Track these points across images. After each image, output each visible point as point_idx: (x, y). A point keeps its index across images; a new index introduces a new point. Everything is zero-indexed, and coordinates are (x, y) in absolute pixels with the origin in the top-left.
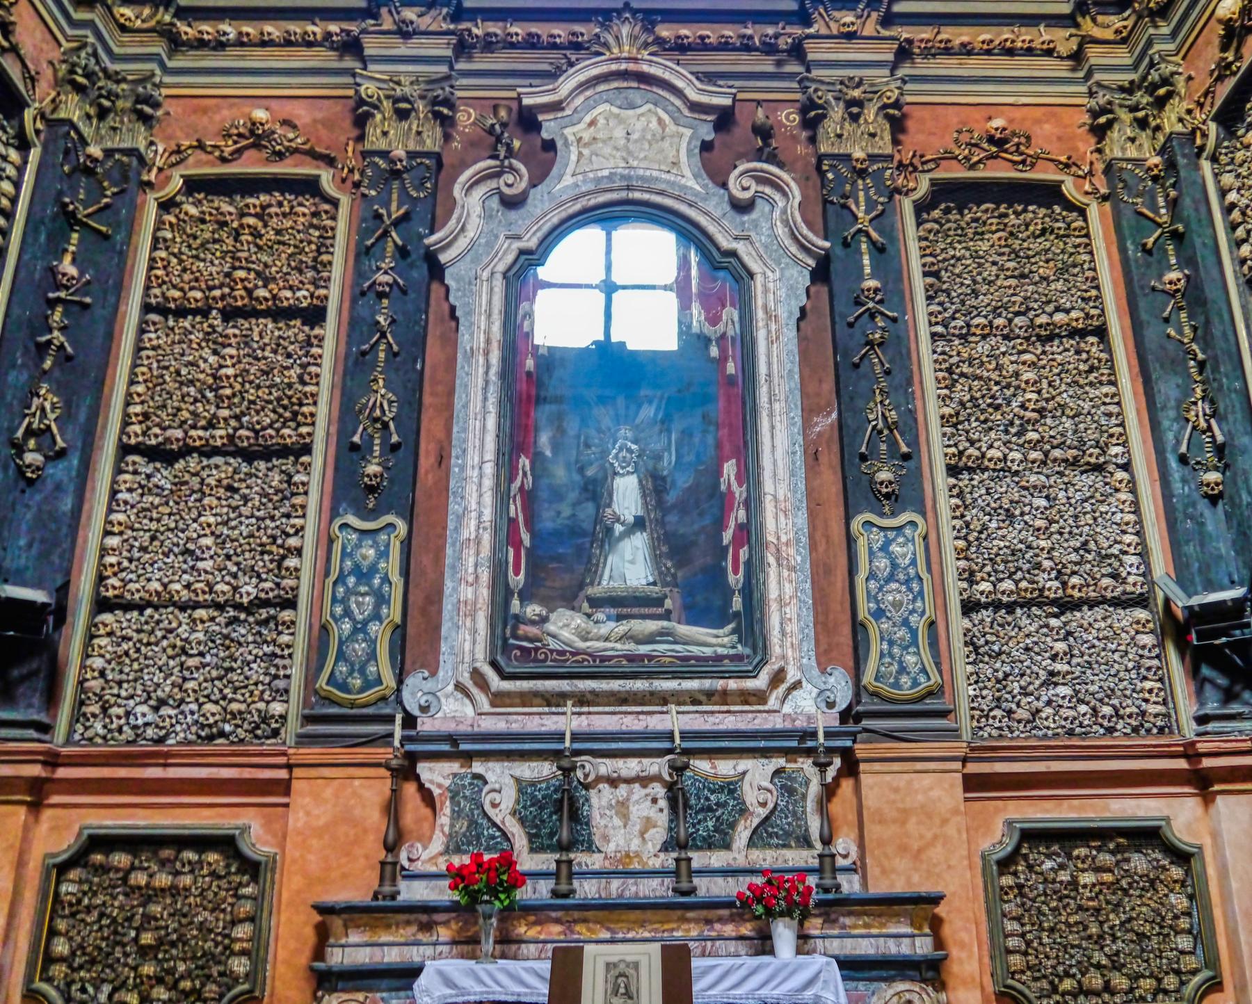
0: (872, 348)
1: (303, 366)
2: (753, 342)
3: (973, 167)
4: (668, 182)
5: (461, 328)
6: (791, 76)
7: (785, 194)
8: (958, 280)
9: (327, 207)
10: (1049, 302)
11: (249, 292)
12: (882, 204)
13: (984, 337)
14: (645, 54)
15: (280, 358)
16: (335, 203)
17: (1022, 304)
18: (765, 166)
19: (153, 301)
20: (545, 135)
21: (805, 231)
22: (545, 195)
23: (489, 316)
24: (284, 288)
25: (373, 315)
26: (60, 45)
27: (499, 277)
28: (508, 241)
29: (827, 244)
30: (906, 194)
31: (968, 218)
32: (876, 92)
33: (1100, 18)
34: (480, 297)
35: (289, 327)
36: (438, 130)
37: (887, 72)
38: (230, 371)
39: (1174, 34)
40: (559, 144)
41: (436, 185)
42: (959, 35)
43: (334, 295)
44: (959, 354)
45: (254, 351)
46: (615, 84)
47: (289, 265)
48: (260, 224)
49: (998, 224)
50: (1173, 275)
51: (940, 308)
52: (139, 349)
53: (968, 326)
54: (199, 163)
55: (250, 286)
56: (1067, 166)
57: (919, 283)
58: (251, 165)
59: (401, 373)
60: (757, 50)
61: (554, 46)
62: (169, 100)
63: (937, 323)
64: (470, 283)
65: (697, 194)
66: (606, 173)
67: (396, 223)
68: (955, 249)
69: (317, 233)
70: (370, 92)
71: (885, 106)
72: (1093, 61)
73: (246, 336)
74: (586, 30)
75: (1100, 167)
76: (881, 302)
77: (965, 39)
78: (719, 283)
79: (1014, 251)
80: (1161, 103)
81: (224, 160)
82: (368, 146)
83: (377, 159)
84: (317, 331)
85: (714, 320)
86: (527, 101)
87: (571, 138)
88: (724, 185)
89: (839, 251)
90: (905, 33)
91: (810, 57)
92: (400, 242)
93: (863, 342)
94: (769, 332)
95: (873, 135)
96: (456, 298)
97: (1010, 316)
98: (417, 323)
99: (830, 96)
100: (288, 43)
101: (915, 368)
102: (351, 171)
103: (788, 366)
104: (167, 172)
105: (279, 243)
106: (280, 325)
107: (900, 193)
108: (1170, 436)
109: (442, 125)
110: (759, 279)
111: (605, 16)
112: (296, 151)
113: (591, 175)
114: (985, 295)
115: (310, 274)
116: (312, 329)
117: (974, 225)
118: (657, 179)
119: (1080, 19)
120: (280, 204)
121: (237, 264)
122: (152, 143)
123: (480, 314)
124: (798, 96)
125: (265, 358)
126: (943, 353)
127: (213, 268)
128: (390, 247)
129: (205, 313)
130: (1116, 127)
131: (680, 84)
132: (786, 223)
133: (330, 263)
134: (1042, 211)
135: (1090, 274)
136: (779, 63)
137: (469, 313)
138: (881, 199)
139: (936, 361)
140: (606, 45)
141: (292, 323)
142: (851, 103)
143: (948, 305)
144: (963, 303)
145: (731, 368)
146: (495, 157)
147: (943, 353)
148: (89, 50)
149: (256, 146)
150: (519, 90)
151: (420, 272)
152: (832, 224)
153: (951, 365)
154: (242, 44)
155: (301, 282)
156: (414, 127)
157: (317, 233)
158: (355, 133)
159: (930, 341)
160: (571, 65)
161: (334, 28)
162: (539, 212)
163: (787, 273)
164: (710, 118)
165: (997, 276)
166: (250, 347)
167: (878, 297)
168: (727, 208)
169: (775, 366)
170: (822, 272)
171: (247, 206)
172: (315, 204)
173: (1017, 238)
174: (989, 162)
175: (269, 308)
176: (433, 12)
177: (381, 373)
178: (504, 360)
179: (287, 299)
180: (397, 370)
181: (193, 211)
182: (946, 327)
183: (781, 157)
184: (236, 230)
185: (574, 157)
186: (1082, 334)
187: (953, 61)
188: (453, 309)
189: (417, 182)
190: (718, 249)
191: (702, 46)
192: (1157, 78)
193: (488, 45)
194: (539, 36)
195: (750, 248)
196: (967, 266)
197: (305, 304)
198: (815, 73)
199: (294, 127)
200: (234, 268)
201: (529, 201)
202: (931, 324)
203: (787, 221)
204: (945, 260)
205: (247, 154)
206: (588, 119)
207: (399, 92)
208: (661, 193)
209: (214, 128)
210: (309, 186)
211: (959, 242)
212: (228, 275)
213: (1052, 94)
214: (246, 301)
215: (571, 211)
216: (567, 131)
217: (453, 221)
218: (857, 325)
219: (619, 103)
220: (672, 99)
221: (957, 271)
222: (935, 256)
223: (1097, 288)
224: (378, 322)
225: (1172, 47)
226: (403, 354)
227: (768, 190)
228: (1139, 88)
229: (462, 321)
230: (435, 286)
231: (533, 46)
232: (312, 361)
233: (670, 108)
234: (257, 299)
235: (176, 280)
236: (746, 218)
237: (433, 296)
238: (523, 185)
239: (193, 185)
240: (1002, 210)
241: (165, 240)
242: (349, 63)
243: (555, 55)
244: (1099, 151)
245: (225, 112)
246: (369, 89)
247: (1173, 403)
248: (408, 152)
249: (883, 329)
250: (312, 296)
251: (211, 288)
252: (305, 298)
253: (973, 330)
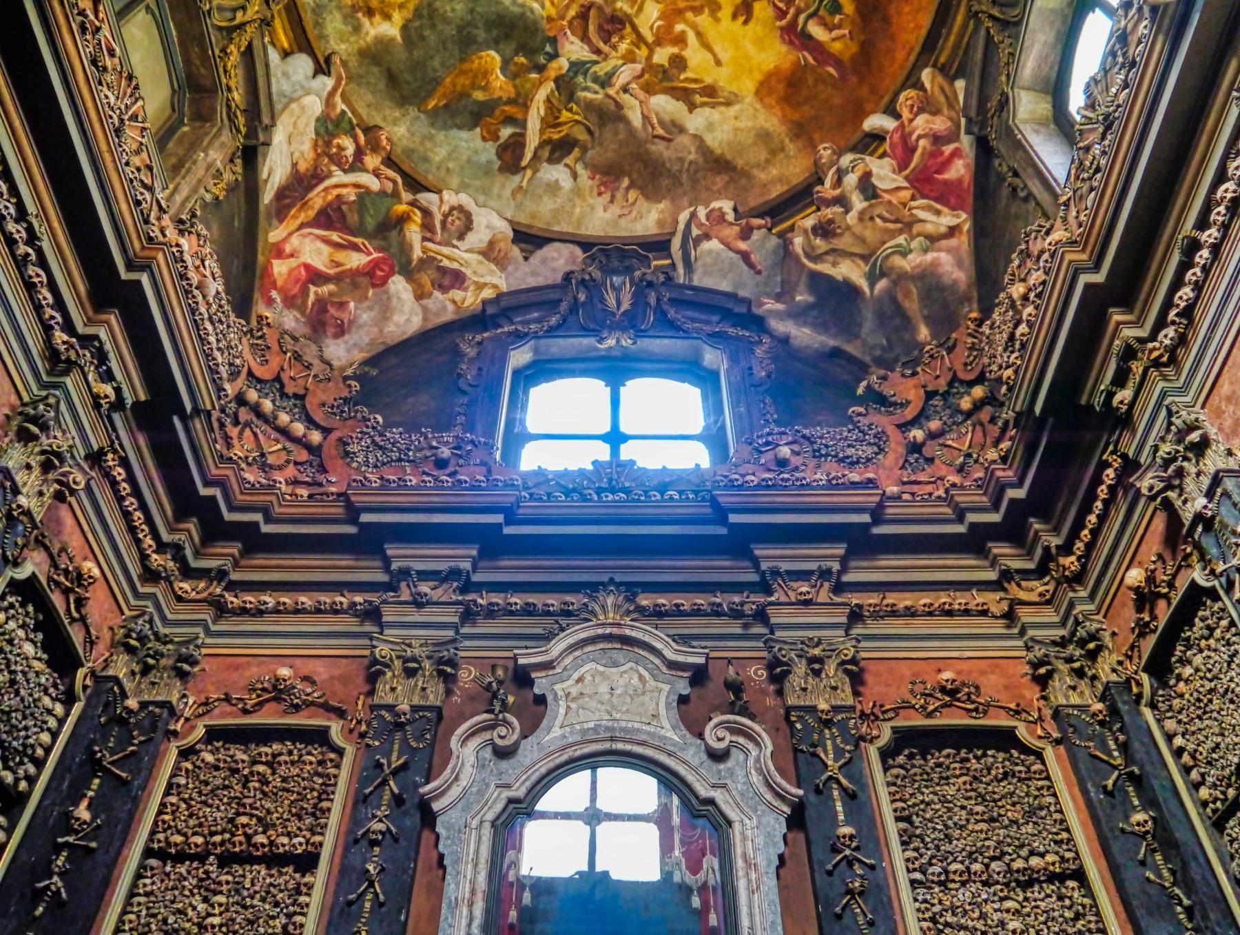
0: (853, 898)
1: (289, 916)
2: (734, 891)
3: (930, 715)
4: (649, 733)
5: (448, 877)
6: (757, 637)
7: (757, 744)
8: (930, 825)
9: (332, 756)
10: (1022, 846)
11: (248, 837)
12: (849, 752)
13: (963, 884)
14: (627, 620)
15: (267, 907)
16: (340, 752)
17: (996, 848)
18: (738, 718)
19: (156, 846)
20: (537, 690)
21: (779, 779)
22: (535, 747)
23: (476, 865)
24: (283, 834)
25: (365, 861)
26: (123, 614)
27: (487, 825)
28: (499, 790)
29: (801, 792)
30: (871, 742)
31: (931, 763)
32: (834, 650)
33: (1023, 583)
34: (468, 845)
35: (281, 874)
36: (441, 687)
37: (842, 633)
38: (216, 920)
39: (1092, 597)
40: (550, 698)
41: (435, 736)
42: (904, 600)
43: (329, 841)
44: (940, 902)
45: (244, 899)
46: (601, 646)
47: (290, 811)
48: (269, 771)
49: (961, 768)
50: (1139, 817)
51: (916, 854)
52: (132, 894)
53: (946, 872)
54: (224, 715)
55: (250, 832)
56: (1017, 712)
57: (892, 829)
58: (268, 717)
59: (385, 924)
60: (725, 615)
61: (548, 614)
62: (207, 658)
63: (915, 870)
64: (460, 831)
65: (675, 744)
66: (591, 725)
67: (395, 773)
68: (923, 794)
69: (320, 781)
70: (383, 653)
71: (843, 663)
72: (1025, 620)
73: (238, 883)
74: (576, 600)
75: (1048, 713)
76: (857, 849)
77: (908, 603)
78: (699, 831)
79: (980, 795)
80: (1093, 656)
81: (245, 712)
82: (377, 701)
83: (383, 713)
84: (308, 879)
85: (695, 868)
86: (521, 661)
87: (560, 693)
88: (700, 736)
89: (812, 798)
90: (855, 599)
91: (773, 620)
92: (396, 791)
93: (843, 890)
94: (749, 881)
95: (835, 688)
96: (445, 846)
97: (986, 861)
98: (405, 872)
99: (793, 654)
100: (318, 611)
101: (898, 918)
102: (359, 722)
103: (771, 917)
104: (192, 723)
105: (284, 790)
106: (273, 872)
107: (865, 741)
109: (445, 682)
110: (737, 827)
111: (592, 588)
112: (312, 704)
113: (578, 727)
114: (958, 840)
115: (309, 821)
116: (303, 876)
117: (938, 770)
118: (638, 730)
119: (1006, 585)
120: (290, 753)
121: (242, 810)
122: (184, 696)
123: (467, 863)
124: (765, 654)
125: (253, 907)
126: (925, 901)
127: (217, 815)
128: (387, 796)
129: (202, 858)
130: (1056, 676)
131: (658, 645)
132: (760, 771)
133: (329, 810)
134: (1001, 756)
135: (1057, 816)
136: (746, 626)
137: (457, 861)
138: (848, 748)
139: (918, 910)
140: (593, 613)
141: (284, 870)
142: (812, 660)
143: (923, 851)
144: (938, 848)
145: (713, 920)
146: (491, 711)
147: (925, 901)
148: (147, 618)
149: (277, 699)
150: (516, 651)
151: (412, 821)
152: (803, 771)
153: (935, 914)
154: (279, 612)
155: (299, 829)
156: (420, 684)
157: (320, 781)
158: (367, 688)
159: (909, 889)
160: (563, 630)
161: (358, 599)
162: (528, 762)
163: (764, 820)
164: (686, 675)
165: (968, 820)
166: (240, 895)
167: (854, 844)
168: (704, 757)
169: (757, 918)
170: (797, 819)
171: (260, 754)
172: (322, 753)
173: (981, 782)
174: (944, 711)
175: (264, 854)
176: (445, 586)
177: (364, 924)
178: (487, 911)
179: (283, 845)
180: (381, 921)
181: (209, 758)
182: (924, 873)
183: (753, 709)
184: (245, 776)
185: (562, 711)
186: (1061, 878)
187: (900, 621)
188: (441, 857)
189: (417, 734)
190: (697, 797)
191: (678, 612)
192: (1084, 634)
193: (491, 612)
194: (535, 605)
195: (727, 796)
196: (937, 811)
197: (299, 851)
198: (779, 634)
199: (313, 683)
200: (238, 814)
201: (520, 751)
202: (908, 871)
203: (761, 769)
204: (915, 805)
205: (267, 707)
206: (576, 676)
207: (409, 653)
208: (642, 743)
209: (243, 683)
210: (319, 737)
211: (926, 787)
212: (231, 821)
213: (993, 649)
214: (244, 847)
215: (558, 761)
216: (557, 687)
217: (448, 770)
218: (836, 873)
219: (604, 662)
220: (652, 658)
221: (928, 816)
222: (905, 801)
223: (1067, 830)
224: (368, 871)
225: (1092, 607)
226: (388, 903)
227: (741, 740)
228: (1070, 642)
229: (449, 869)
230: (426, 834)
231: (530, 614)
232: (299, 910)
233: (650, 666)
234: (255, 845)
235: (181, 825)
236: (722, 766)
237: (423, 842)
238: (515, 737)
239: (213, 735)
240: (963, 753)
241: (179, 786)
242: (369, 627)
243: (549, 620)
244: (1044, 698)
245: (255, 669)
246: (383, 650)
248: (412, 707)
249: (862, 877)
250: (307, 842)
251: (212, 834)
252: (301, 844)
253: (952, 876)
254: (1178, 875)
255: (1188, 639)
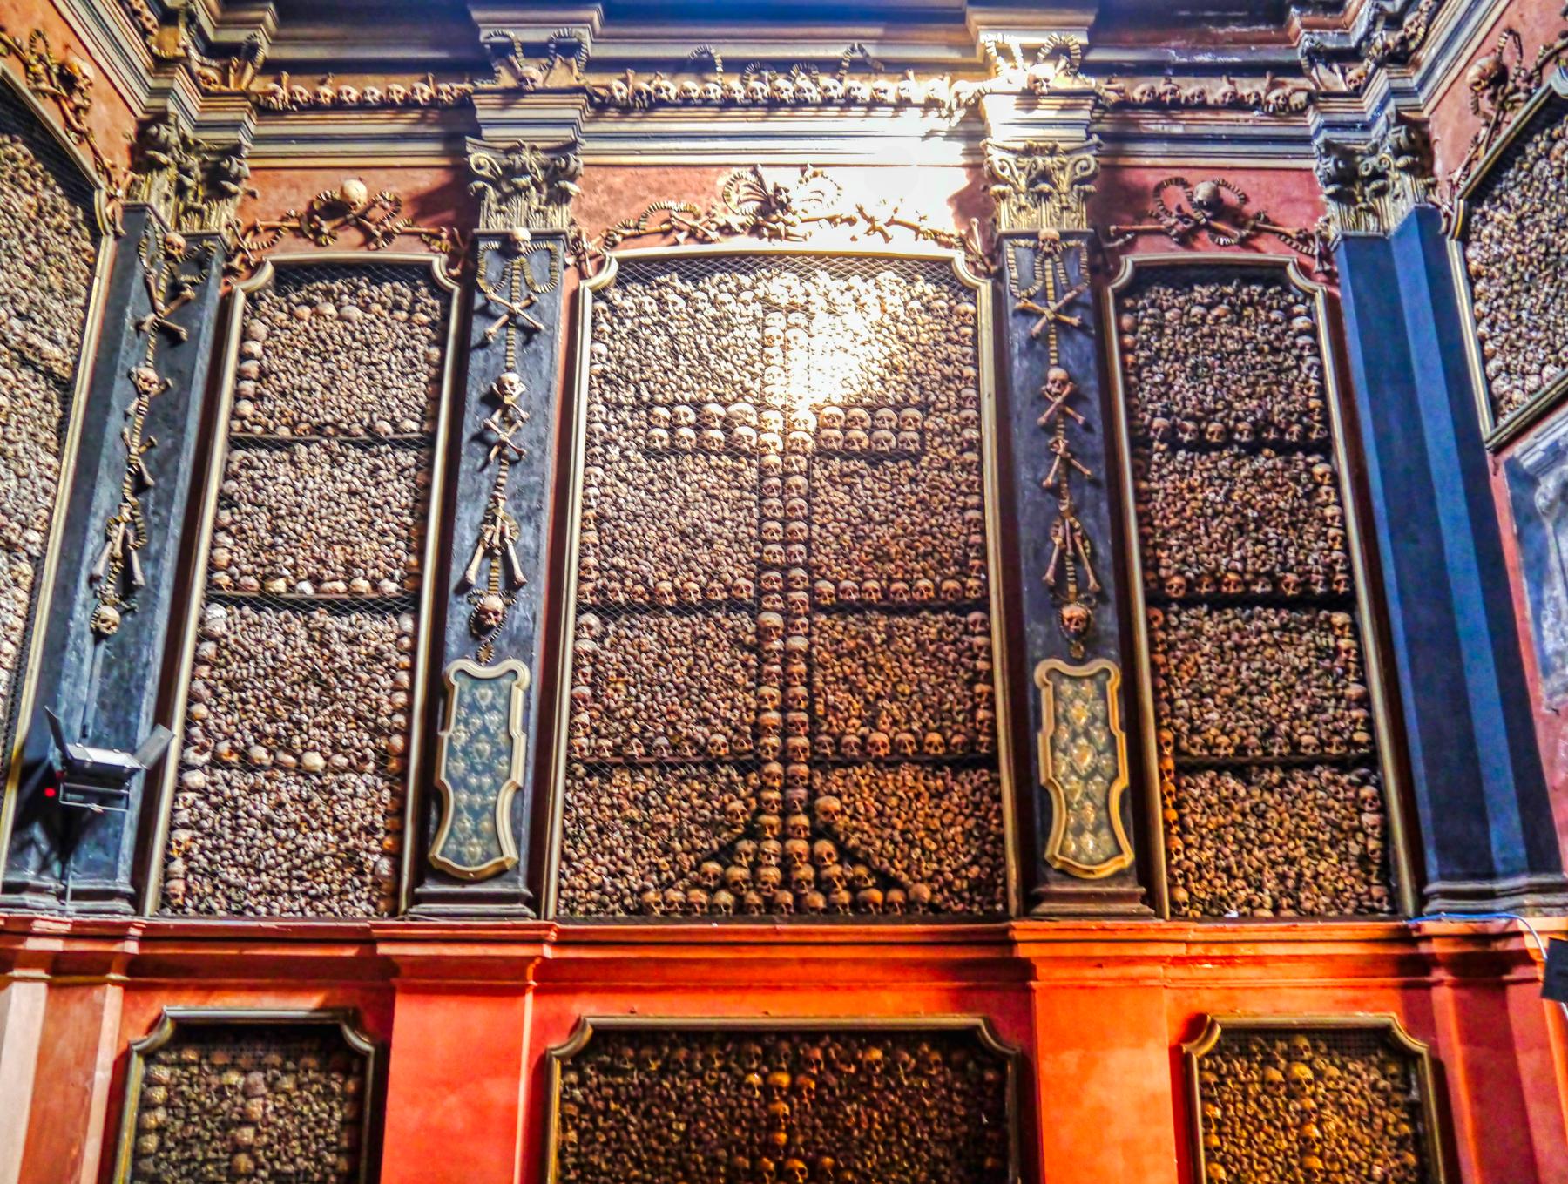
3: (36, 91)
72: (177, 87)
108: (90, 549)
228: (198, 154)
247: (102, 513)
254: (154, 452)
255: (358, 288)
